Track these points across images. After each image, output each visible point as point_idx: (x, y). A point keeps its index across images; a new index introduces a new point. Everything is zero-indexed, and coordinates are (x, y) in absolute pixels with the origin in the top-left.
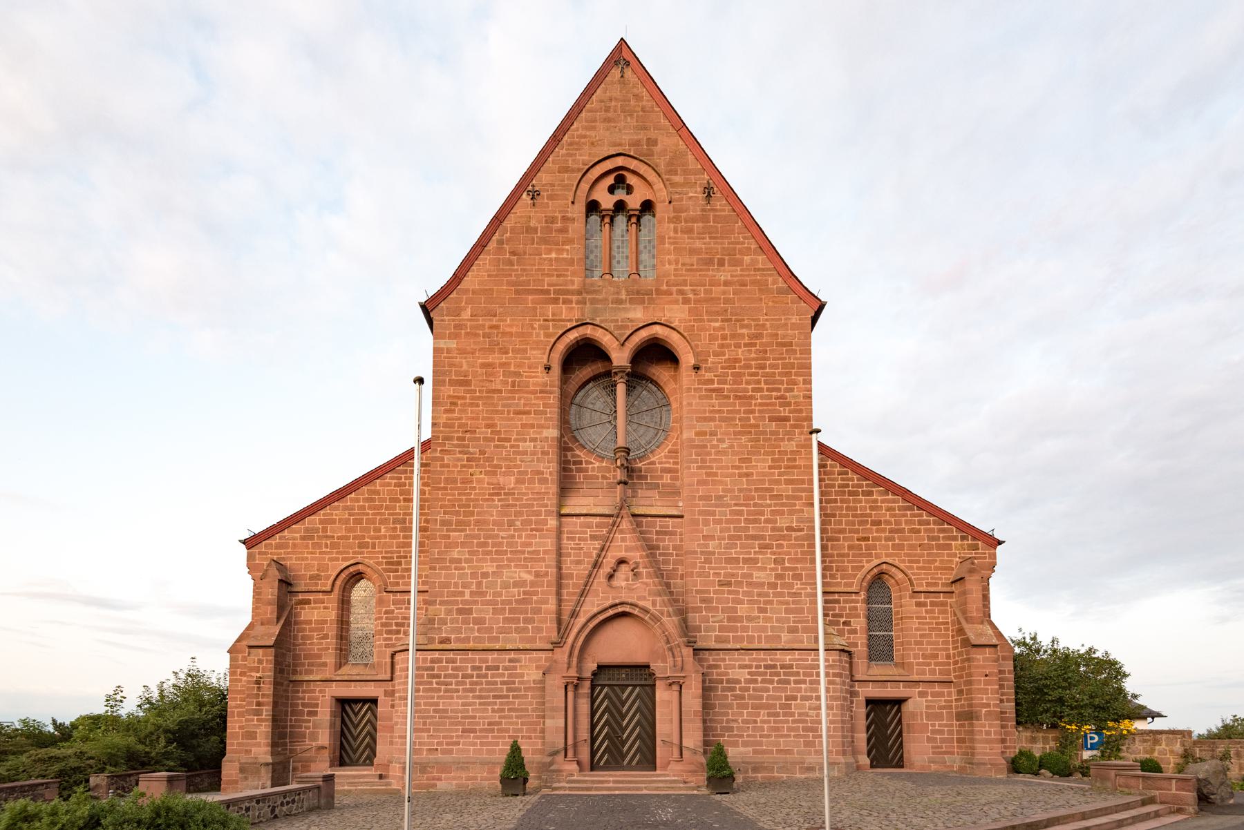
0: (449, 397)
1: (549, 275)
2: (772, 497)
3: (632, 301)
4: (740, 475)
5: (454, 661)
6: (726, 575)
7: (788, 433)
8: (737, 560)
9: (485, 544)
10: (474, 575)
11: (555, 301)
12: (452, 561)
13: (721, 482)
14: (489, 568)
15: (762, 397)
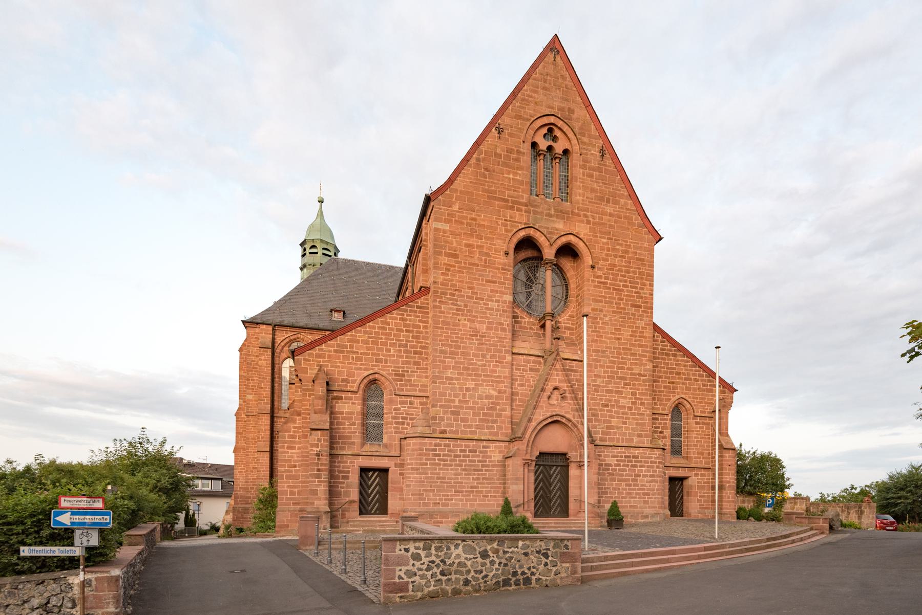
0: (445, 264)
1: (508, 189)
11: (512, 208)
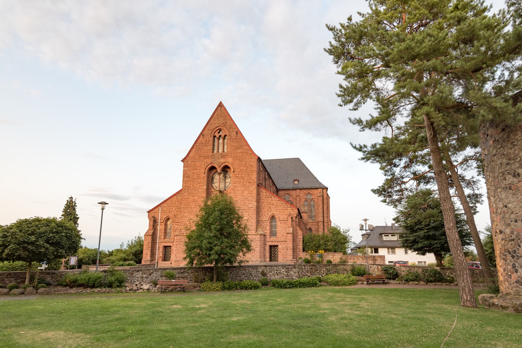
9: (191, 212)
11: (206, 158)
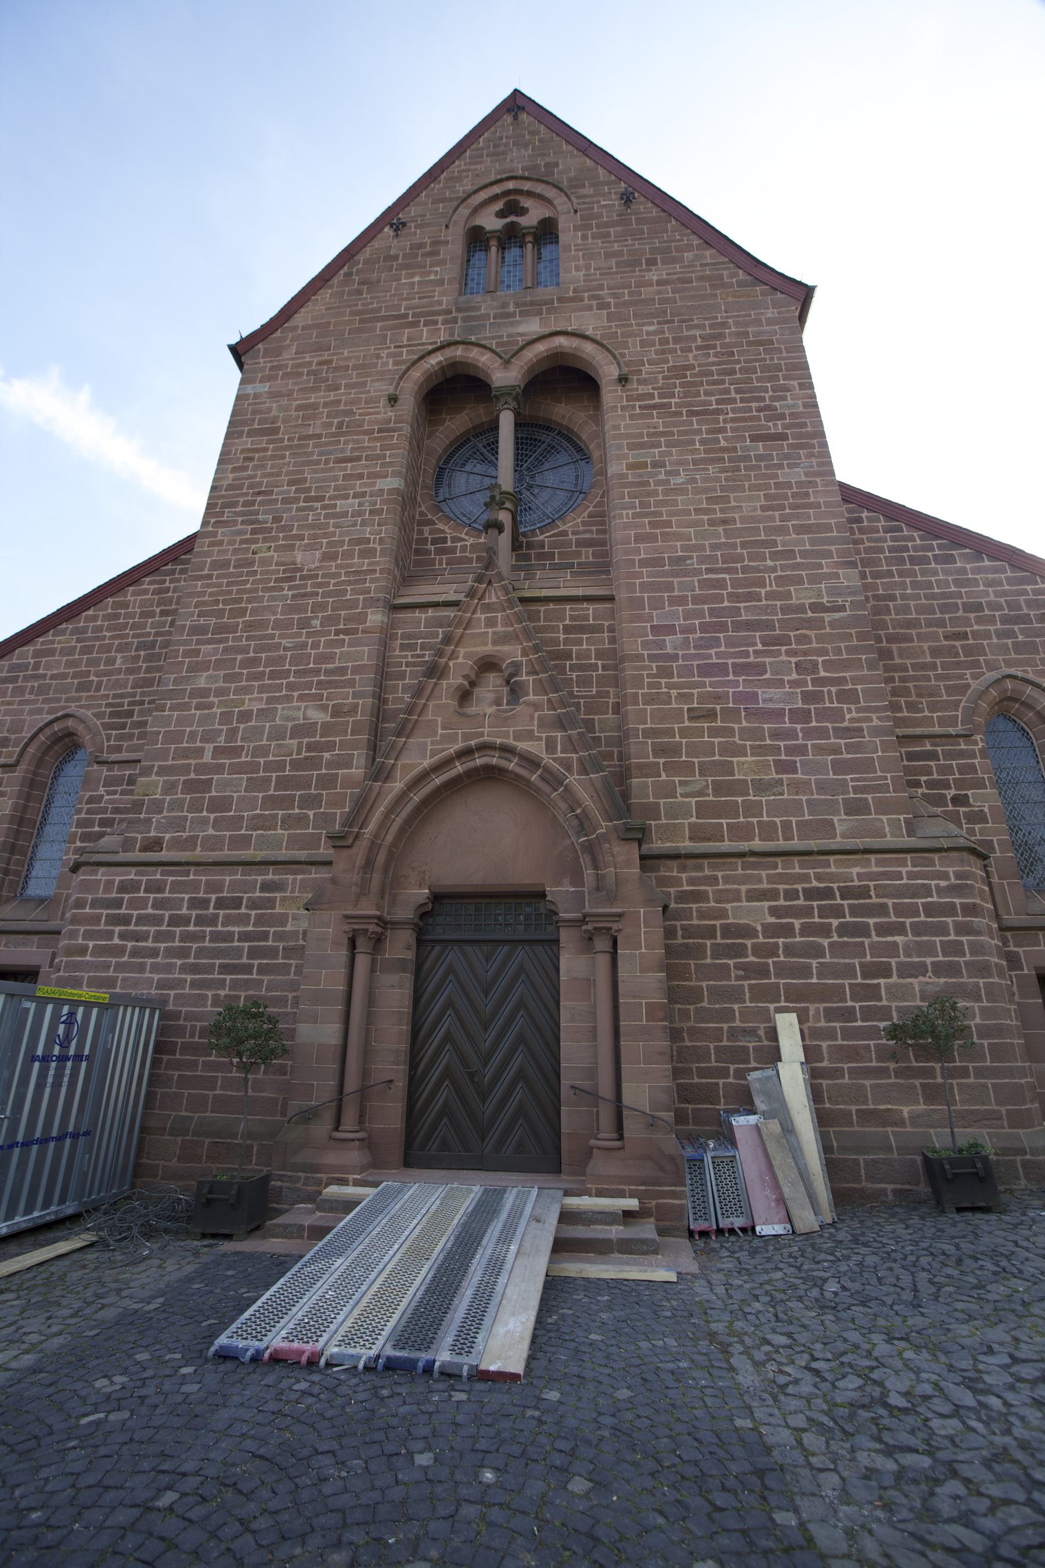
2: (774, 556)
3: (523, 314)
4: (712, 523)
5: (159, 887)
6: (703, 698)
7: (787, 456)
8: (722, 669)
9: (255, 662)
10: (226, 718)
11: (415, 324)
12: (195, 693)
13: (679, 536)
14: (253, 703)
15: (733, 410)
